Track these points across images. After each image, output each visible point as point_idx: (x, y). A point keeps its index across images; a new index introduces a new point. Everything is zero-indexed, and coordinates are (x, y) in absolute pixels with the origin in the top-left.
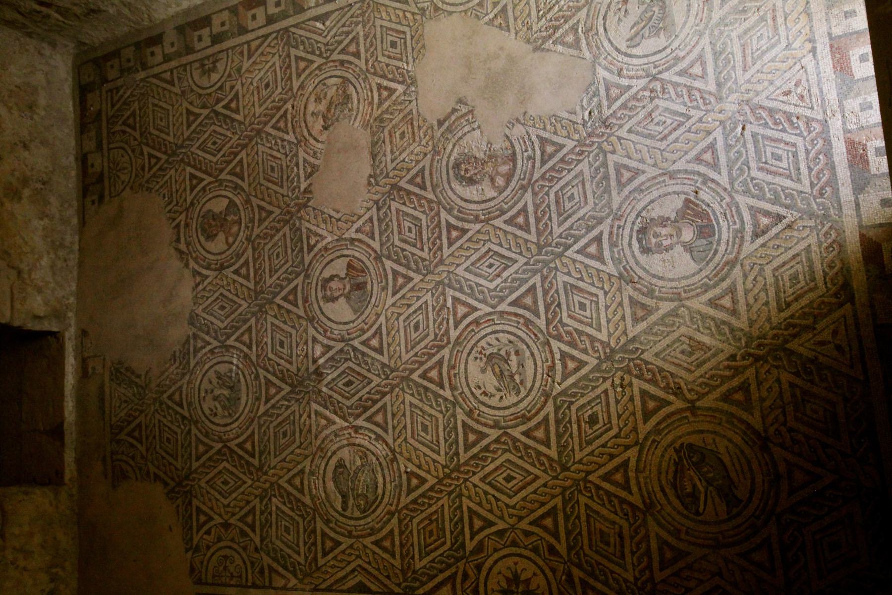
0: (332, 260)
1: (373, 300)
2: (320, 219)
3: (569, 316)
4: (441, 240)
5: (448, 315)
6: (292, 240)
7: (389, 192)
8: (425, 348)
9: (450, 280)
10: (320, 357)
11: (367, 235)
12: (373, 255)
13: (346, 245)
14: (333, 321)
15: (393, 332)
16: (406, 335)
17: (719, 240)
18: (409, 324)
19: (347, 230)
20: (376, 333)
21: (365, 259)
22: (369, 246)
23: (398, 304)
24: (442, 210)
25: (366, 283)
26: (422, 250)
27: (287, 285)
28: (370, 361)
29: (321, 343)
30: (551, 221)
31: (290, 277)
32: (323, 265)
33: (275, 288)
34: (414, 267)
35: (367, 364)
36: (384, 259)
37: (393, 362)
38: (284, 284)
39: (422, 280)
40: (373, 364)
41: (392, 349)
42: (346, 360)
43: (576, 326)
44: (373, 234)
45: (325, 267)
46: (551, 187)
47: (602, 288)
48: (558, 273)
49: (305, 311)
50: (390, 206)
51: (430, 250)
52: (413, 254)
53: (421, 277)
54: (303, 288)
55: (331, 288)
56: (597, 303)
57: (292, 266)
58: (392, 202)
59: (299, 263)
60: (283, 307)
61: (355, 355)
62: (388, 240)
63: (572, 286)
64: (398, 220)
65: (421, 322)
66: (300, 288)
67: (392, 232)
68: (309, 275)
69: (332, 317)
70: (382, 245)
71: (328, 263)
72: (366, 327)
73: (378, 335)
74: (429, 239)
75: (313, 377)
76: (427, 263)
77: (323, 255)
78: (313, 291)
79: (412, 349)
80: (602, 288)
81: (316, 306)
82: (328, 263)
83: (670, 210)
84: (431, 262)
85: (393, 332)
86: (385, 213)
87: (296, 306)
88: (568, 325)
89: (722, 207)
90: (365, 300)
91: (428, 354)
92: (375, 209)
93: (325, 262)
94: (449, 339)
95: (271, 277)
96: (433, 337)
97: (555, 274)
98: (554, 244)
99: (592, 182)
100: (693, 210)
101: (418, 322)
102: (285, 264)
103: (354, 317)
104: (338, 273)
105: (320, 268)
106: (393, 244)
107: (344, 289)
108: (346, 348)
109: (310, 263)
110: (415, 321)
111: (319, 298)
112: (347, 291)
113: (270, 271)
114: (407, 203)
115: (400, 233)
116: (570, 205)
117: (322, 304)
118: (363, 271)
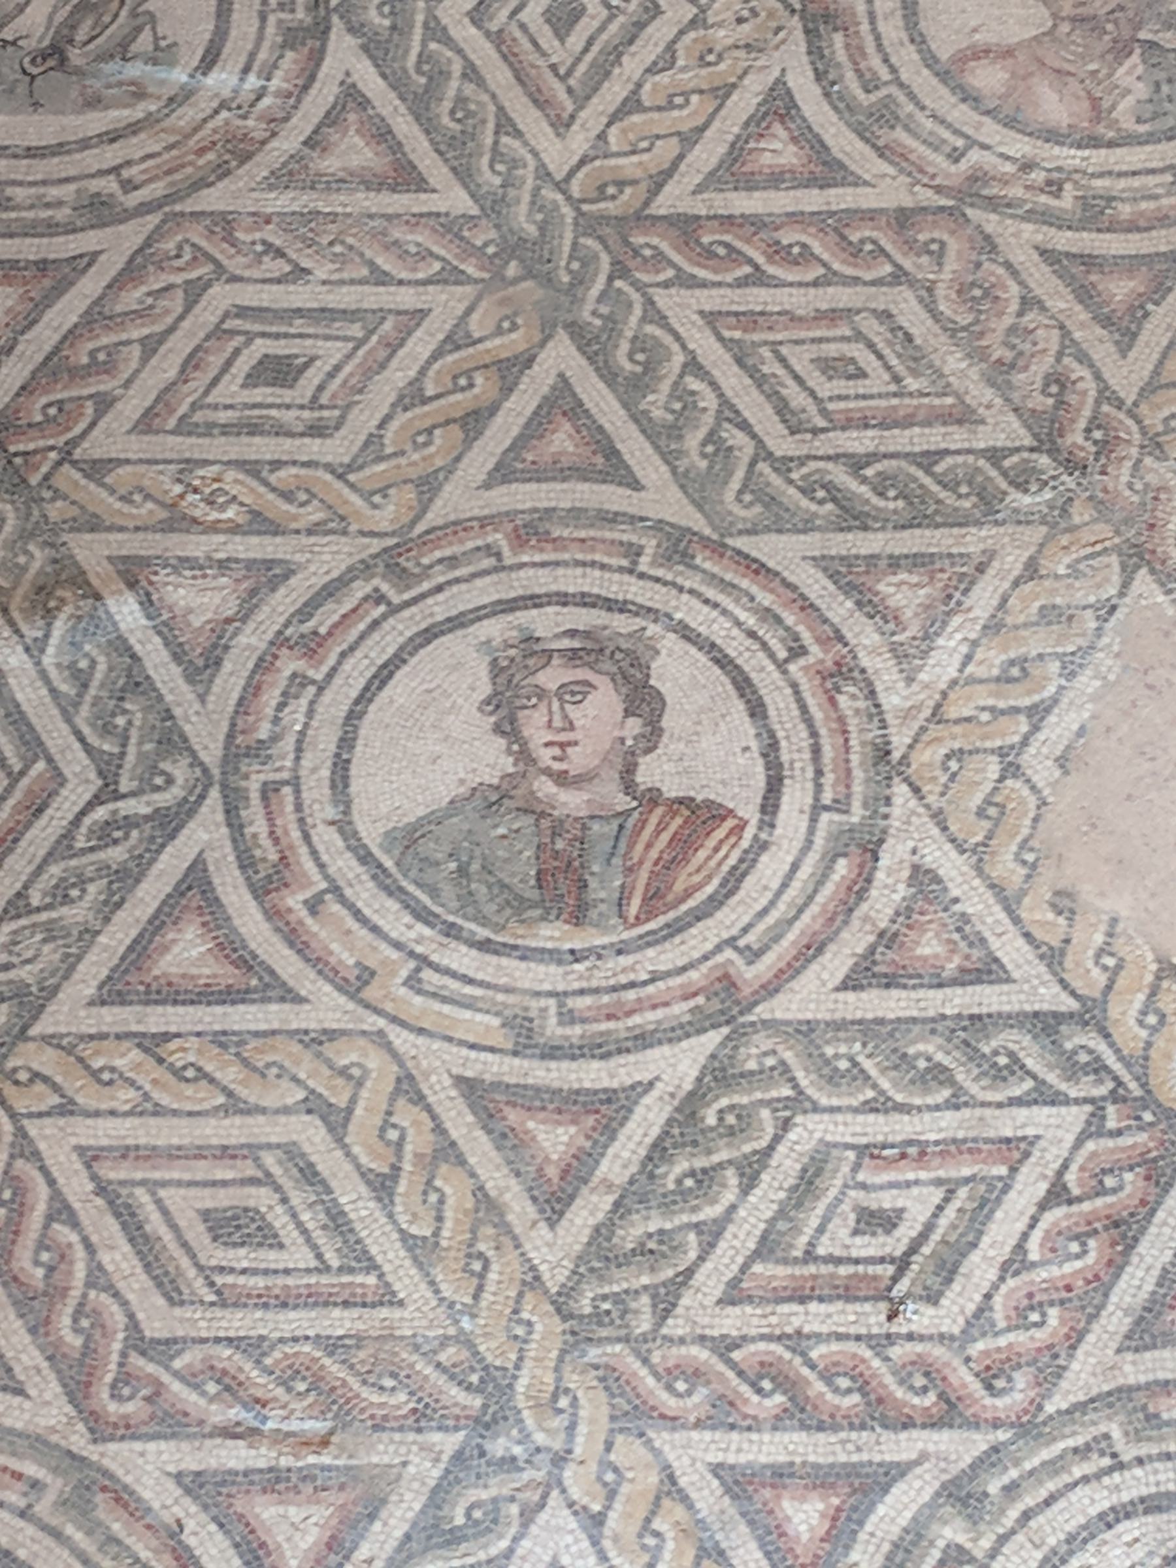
0: (757, 710)
1: (461, 958)
2: (1035, 644)
4: (778, 1423)
5: (280, 1438)
6: (928, 459)
7: (1148, 1099)
8: (98, 1277)
9: (510, 1463)
10: (147, 603)
11: (888, 939)
12: (751, 974)
13: (841, 805)
14: (366, 697)
15: (230, 1075)
16: (199, 1153)
18: (267, 1180)
19: (939, 818)
20: (246, 962)
21: (729, 919)
22: (812, 949)
23: (406, 1115)
24: (980, 1442)
25: (578, 917)
26: (733, 1295)
27: (640, 419)
28: (75, 914)
29: (244, 616)
31: (693, 440)
32: (736, 646)
33: (639, 343)
34: (631, 1234)
35: (61, 895)
36: (712, 1039)
37: (45, 1060)
38: (656, 404)
39: (533, 1280)
40: (51, 932)
41: (127, 1059)
42: (108, 770)
44: (890, 981)
45: (723, 661)
49: (458, 527)
50: (1056, 1099)
51: (725, 1346)
52: (711, 1234)
53: (554, 1280)
54: (612, 519)
55: (579, 691)
57: (762, 452)
58: (1076, 1117)
59: (770, 501)
60: (508, 390)
61: (130, 823)
62: (833, 1079)
64: (953, 1148)
65: (271, 1258)
66: (613, 497)
67: (880, 1106)
68: (686, 558)
69: (399, 689)
70: (806, 1030)
71: (743, 685)
72: (294, 901)
73: (227, 974)
74: (797, 1340)
75: (39, 557)
76: (643, 1324)
77: (798, 651)
78: (572, 581)
79: (102, 1189)
81: (485, 592)
82: (743, 685)
84: (640, 1346)
85: (230, 1075)
86: (1016, 1065)
87: (502, 473)
90: (467, 899)
91: (55, 1293)
92: (1052, 998)
93: (754, 663)
94: (127, 1430)
95: (711, 318)
96: (153, 1328)
101: (269, 1238)
102: (782, 409)
103: (371, 834)
104: (669, 746)
105: (718, 630)
106: (800, 1102)
107: (561, 779)
108: (180, 770)
109: (757, 569)
110: (279, 1219)
111: (523, 617)
112: (545, 787)
113: (751, 319)
114: (1055, 1215)
115: (868, 1152)
117: (494, 629)
118: (654, 900)
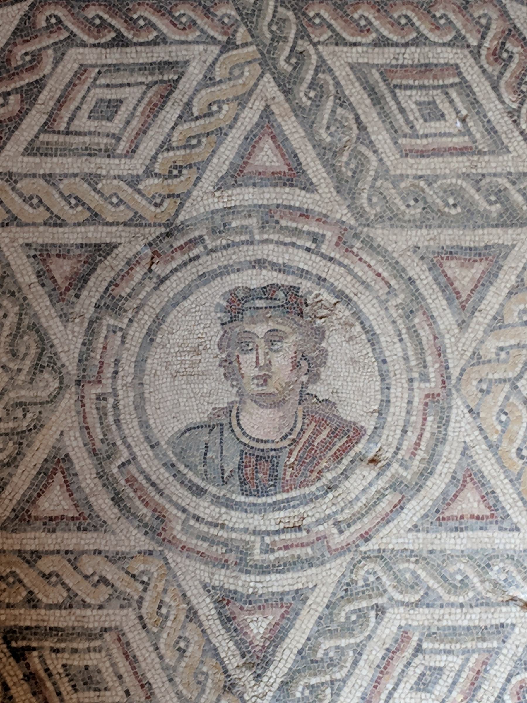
3: (83, 69)
17: (230, 504)
30: (375, 44)
43: (51, 83)
46: (476, 54)
47: (149, 173)
48: (215, 50)
56: (109, 153)
63: (173, 85)
80: (149, 173)
83: (338, 384)
88: (57, 62)
89: (318, 522)
97: (214, 40)
98: (303, 45)
99: (466, 176)
100: (327, 446)
116: (410, 106)
